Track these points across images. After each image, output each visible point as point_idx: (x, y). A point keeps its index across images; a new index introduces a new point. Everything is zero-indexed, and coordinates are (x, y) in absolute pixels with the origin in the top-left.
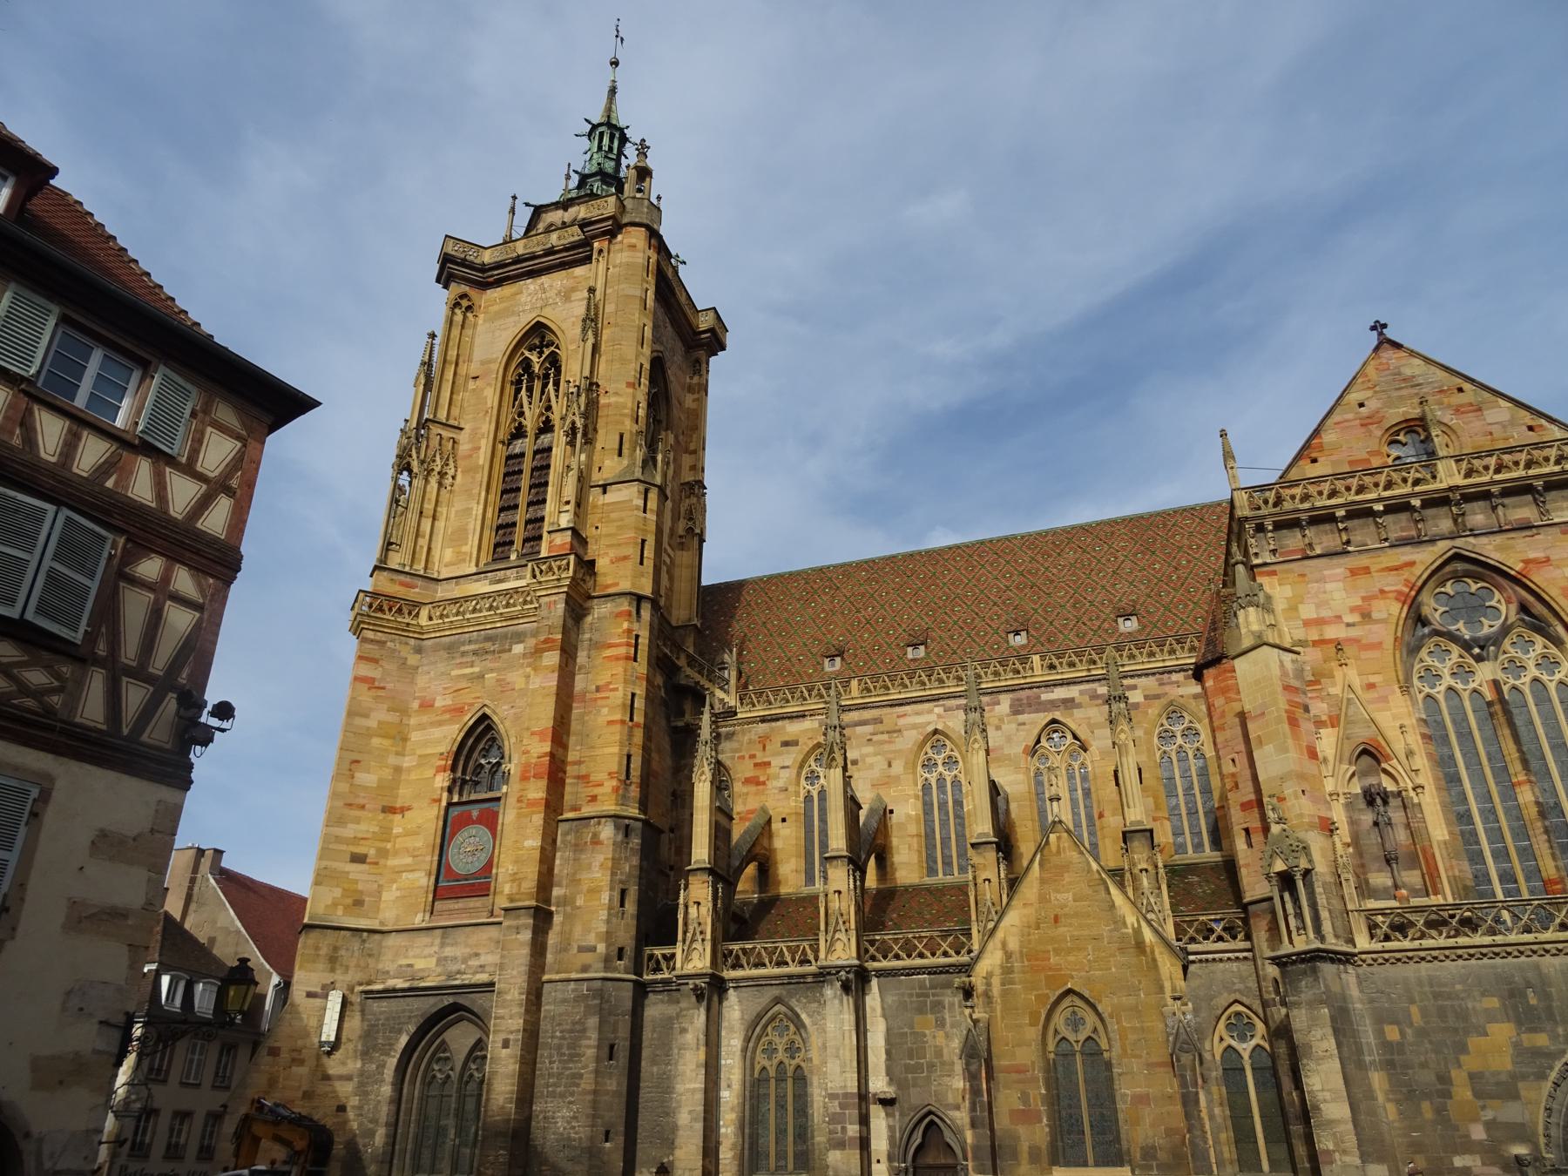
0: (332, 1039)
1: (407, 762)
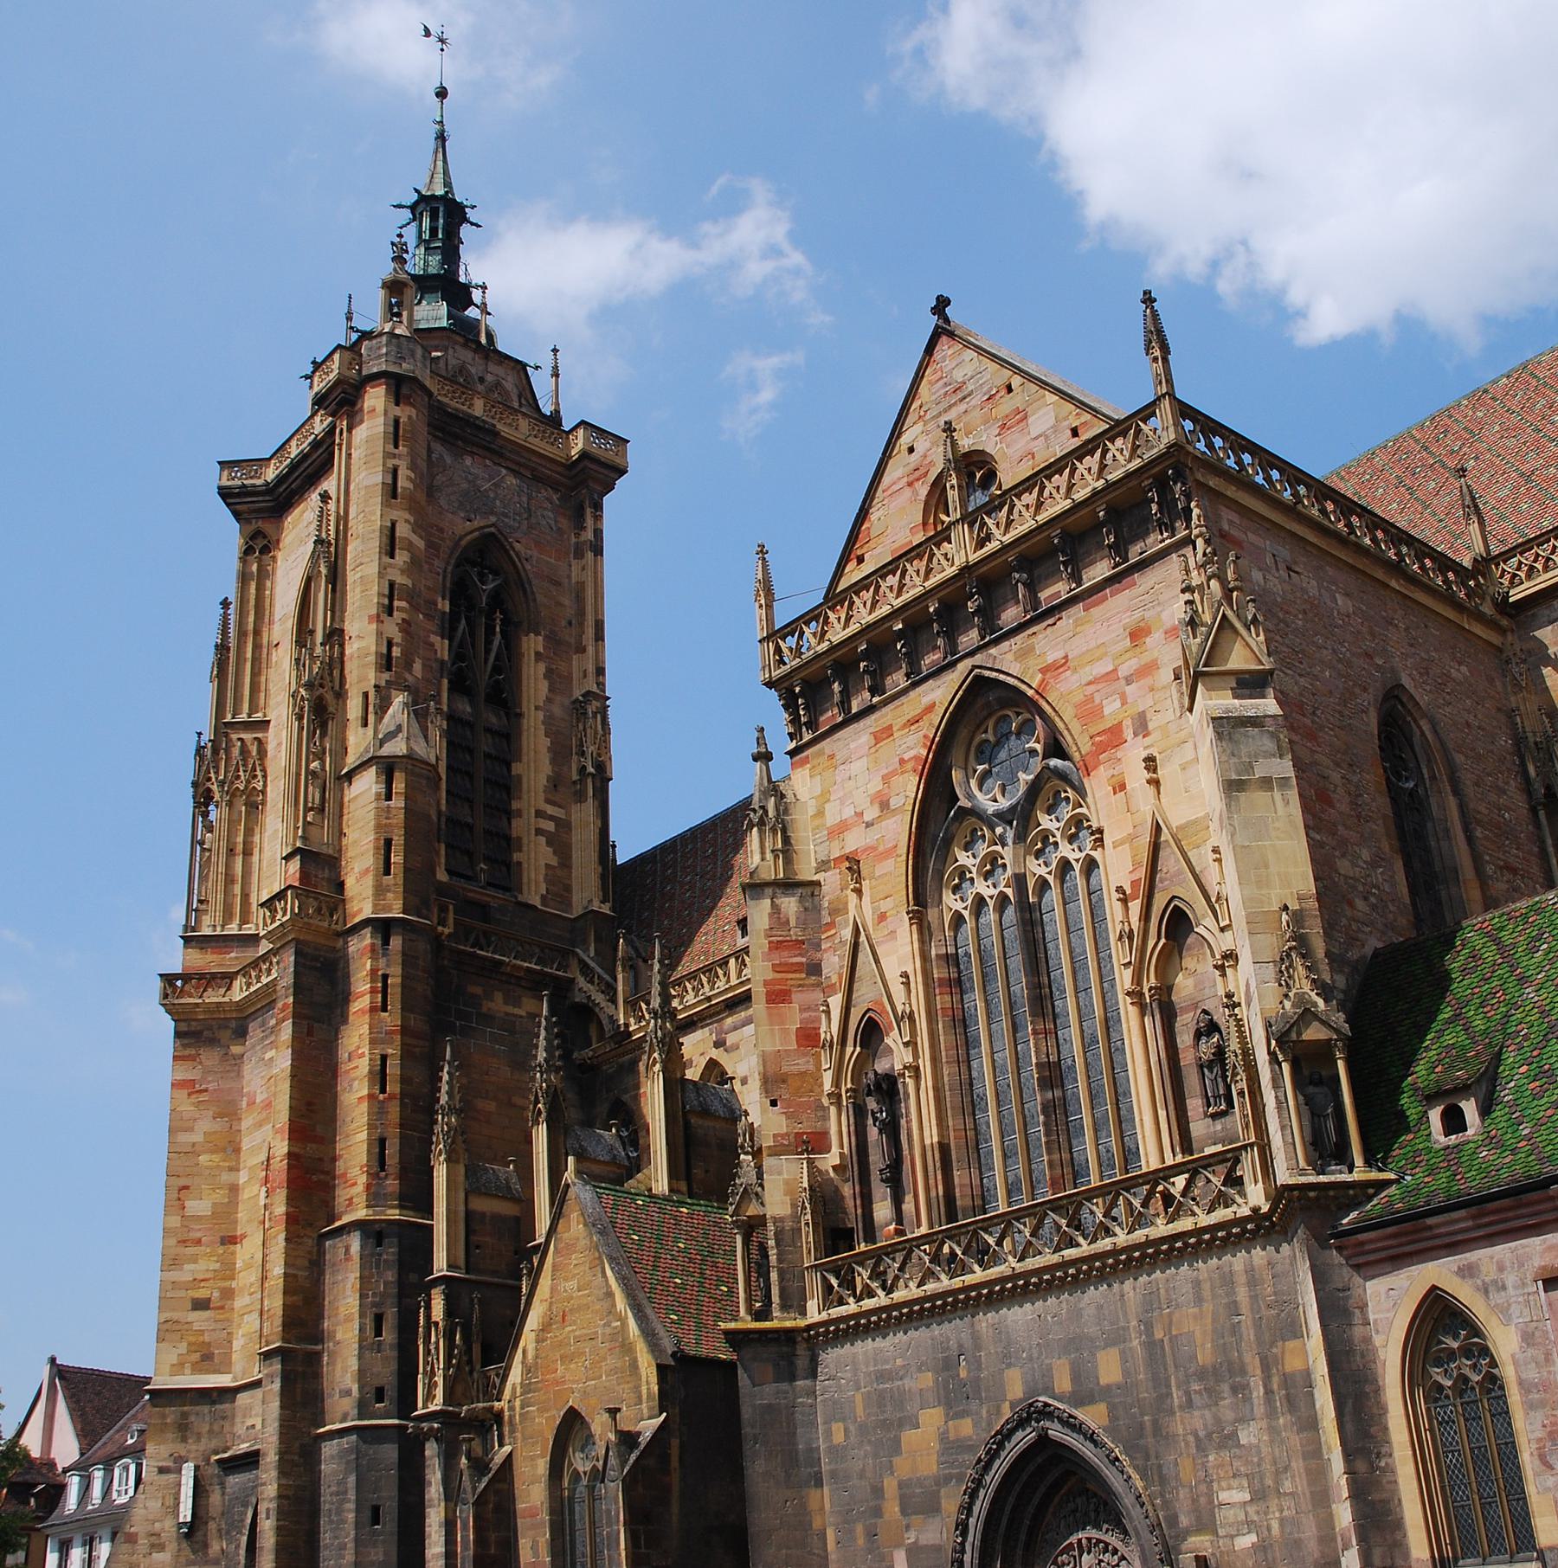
0: (189, 1519)
1: (243, 1177)
